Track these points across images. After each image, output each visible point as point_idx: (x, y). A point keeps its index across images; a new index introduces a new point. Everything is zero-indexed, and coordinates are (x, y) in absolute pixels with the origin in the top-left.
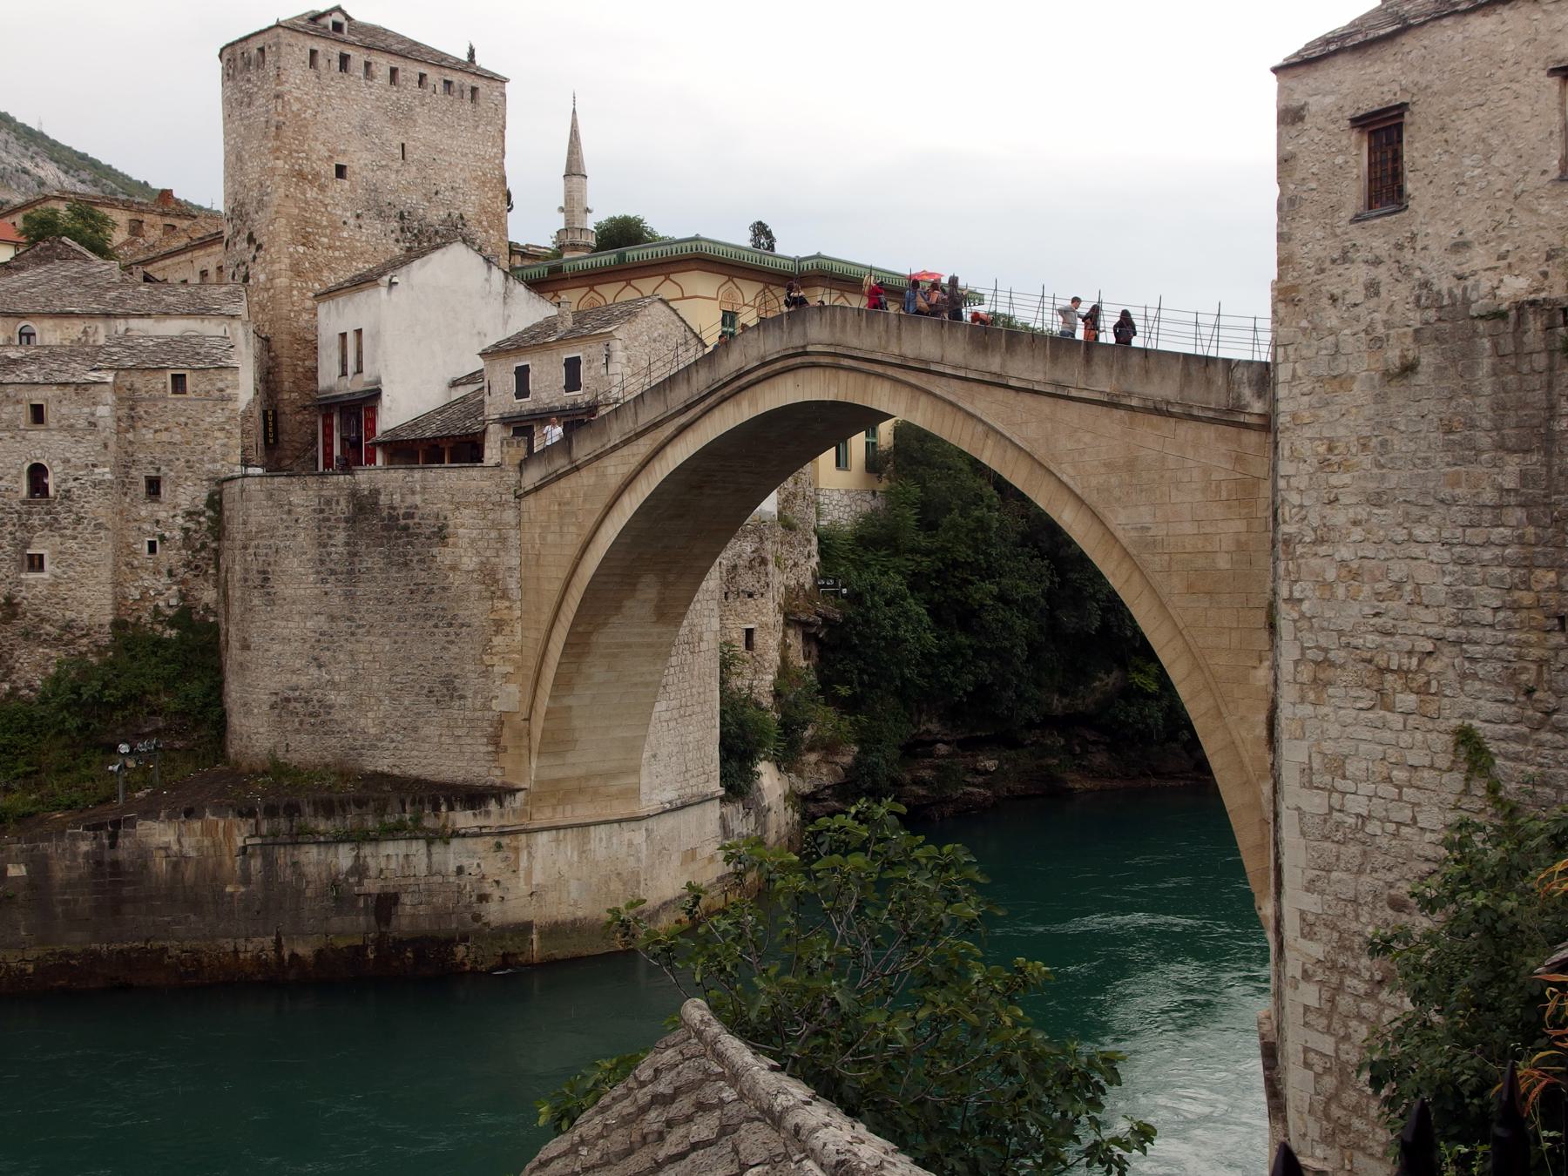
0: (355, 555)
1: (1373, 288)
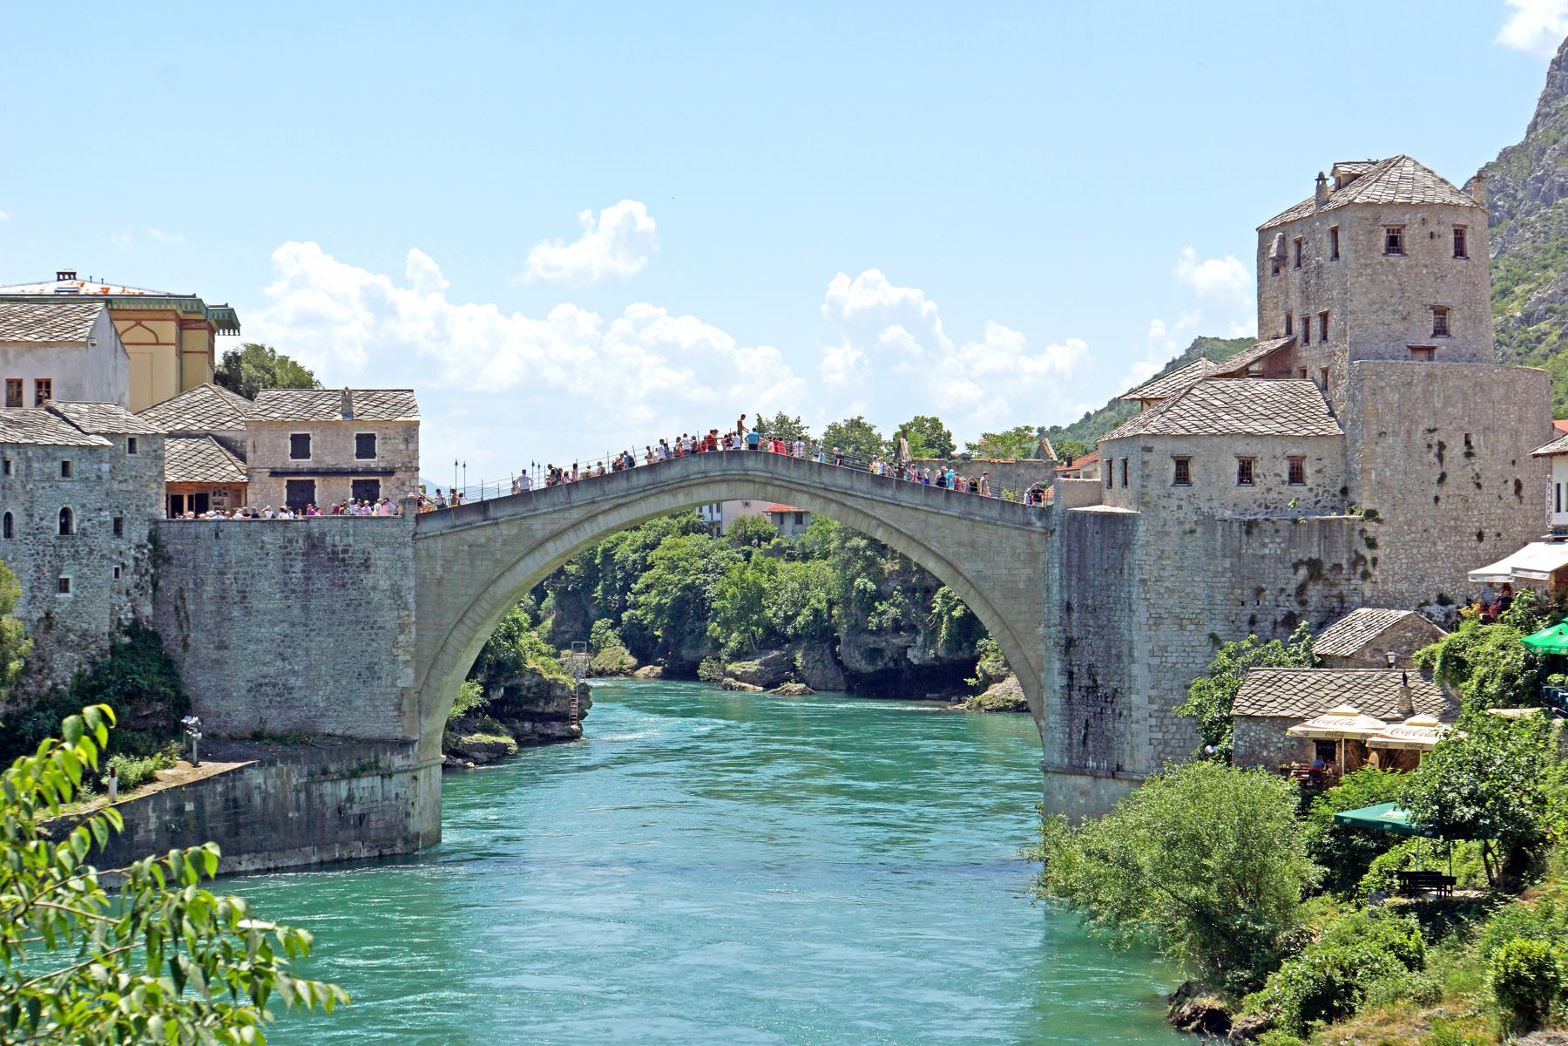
0: (309, 579)
1: (1180, 507)
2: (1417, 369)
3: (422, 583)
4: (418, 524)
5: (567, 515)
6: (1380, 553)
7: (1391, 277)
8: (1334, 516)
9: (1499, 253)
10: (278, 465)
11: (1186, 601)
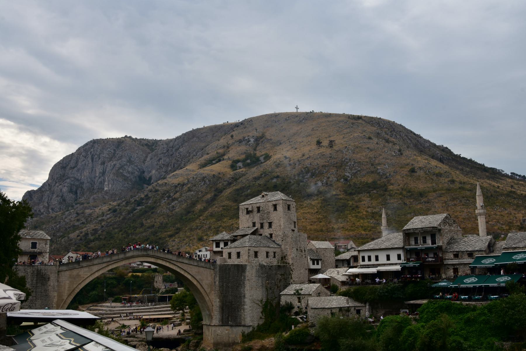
1: (256, 263)
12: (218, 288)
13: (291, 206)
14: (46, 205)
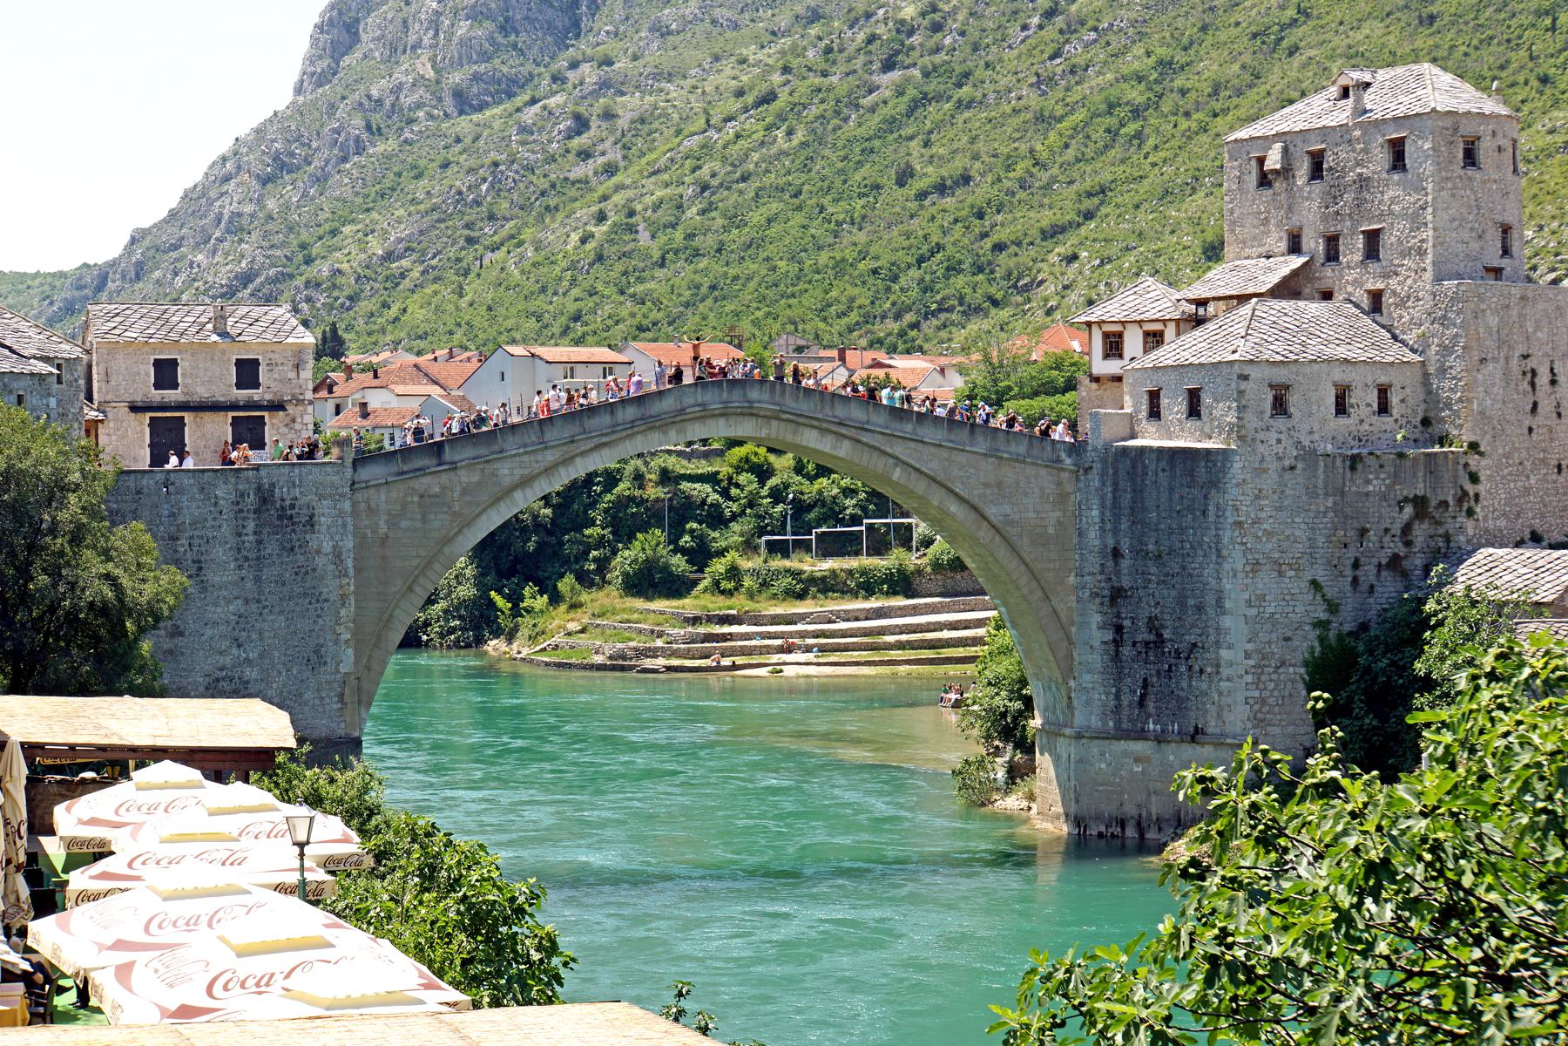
1: (1279, 441)
2: (1513, 291)
3: (361, 545)
4: (355, 469)
5: (539, 457)
6: (1482, 488)
7: (1468, 192)
8: (1437, 449)
9: (302, 196)
10: (138, 398)
11: (1286, 544)
12: (1093, 563)
13: (1485, 149)
14: (430, 74)
